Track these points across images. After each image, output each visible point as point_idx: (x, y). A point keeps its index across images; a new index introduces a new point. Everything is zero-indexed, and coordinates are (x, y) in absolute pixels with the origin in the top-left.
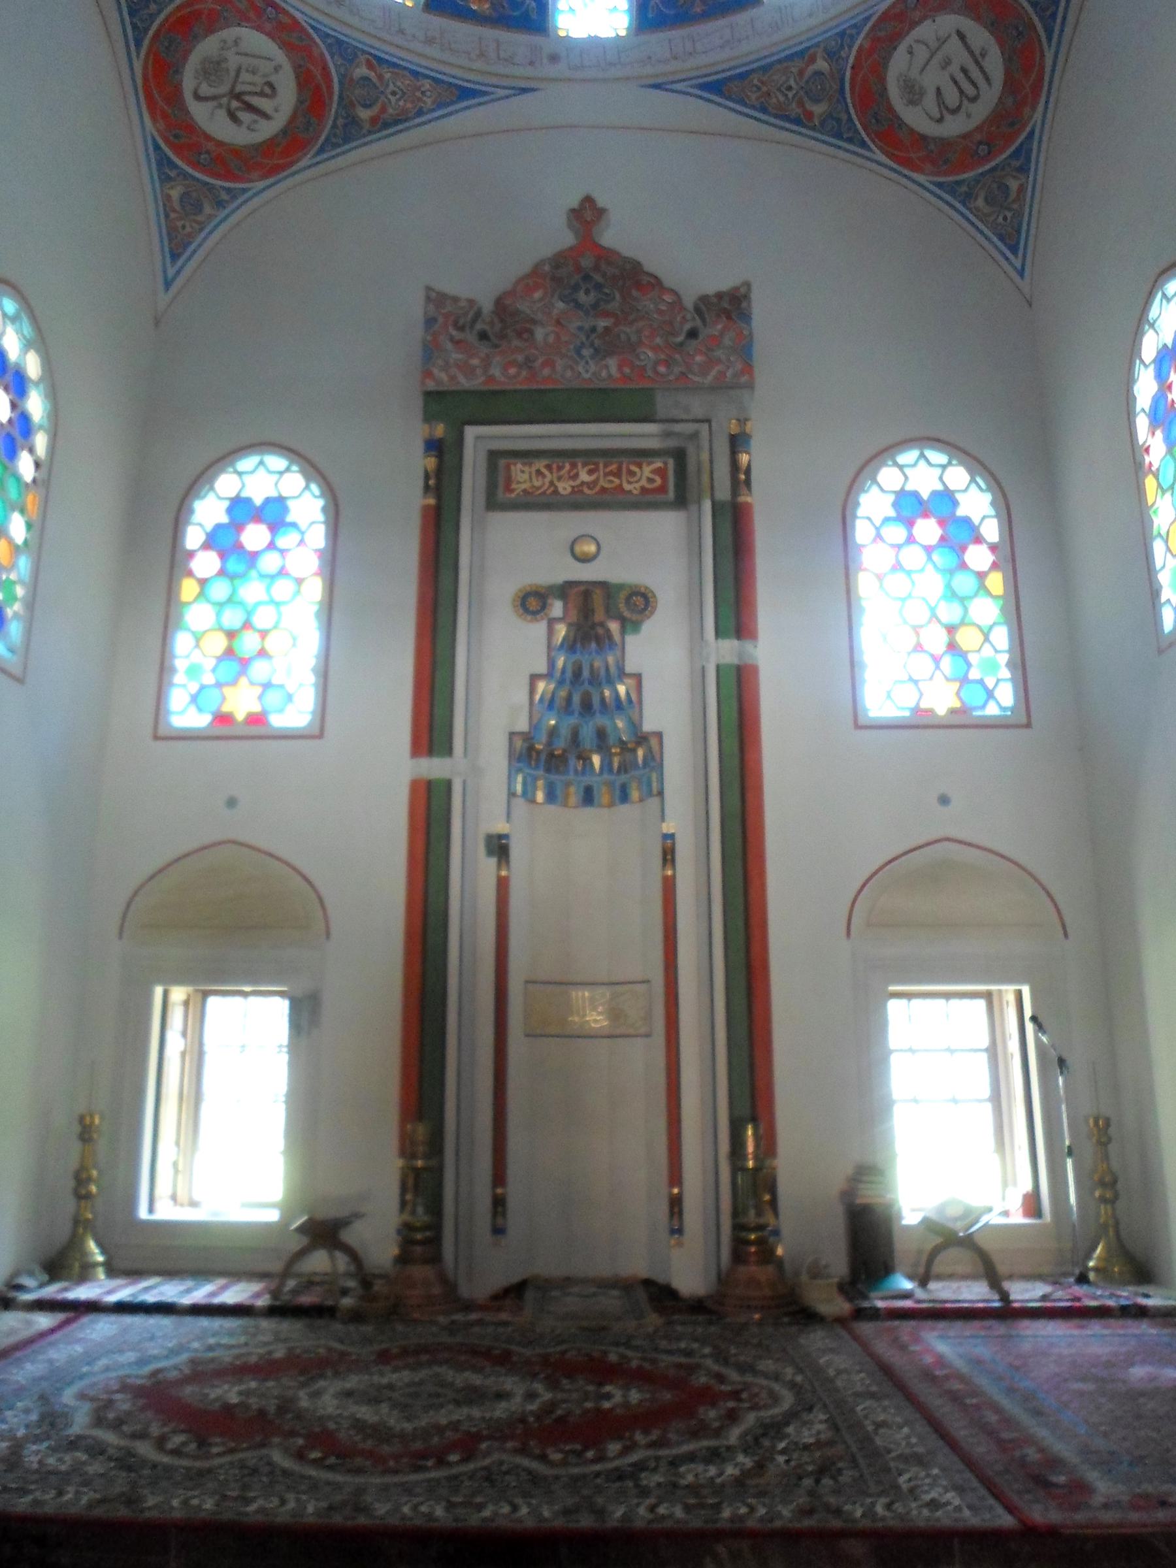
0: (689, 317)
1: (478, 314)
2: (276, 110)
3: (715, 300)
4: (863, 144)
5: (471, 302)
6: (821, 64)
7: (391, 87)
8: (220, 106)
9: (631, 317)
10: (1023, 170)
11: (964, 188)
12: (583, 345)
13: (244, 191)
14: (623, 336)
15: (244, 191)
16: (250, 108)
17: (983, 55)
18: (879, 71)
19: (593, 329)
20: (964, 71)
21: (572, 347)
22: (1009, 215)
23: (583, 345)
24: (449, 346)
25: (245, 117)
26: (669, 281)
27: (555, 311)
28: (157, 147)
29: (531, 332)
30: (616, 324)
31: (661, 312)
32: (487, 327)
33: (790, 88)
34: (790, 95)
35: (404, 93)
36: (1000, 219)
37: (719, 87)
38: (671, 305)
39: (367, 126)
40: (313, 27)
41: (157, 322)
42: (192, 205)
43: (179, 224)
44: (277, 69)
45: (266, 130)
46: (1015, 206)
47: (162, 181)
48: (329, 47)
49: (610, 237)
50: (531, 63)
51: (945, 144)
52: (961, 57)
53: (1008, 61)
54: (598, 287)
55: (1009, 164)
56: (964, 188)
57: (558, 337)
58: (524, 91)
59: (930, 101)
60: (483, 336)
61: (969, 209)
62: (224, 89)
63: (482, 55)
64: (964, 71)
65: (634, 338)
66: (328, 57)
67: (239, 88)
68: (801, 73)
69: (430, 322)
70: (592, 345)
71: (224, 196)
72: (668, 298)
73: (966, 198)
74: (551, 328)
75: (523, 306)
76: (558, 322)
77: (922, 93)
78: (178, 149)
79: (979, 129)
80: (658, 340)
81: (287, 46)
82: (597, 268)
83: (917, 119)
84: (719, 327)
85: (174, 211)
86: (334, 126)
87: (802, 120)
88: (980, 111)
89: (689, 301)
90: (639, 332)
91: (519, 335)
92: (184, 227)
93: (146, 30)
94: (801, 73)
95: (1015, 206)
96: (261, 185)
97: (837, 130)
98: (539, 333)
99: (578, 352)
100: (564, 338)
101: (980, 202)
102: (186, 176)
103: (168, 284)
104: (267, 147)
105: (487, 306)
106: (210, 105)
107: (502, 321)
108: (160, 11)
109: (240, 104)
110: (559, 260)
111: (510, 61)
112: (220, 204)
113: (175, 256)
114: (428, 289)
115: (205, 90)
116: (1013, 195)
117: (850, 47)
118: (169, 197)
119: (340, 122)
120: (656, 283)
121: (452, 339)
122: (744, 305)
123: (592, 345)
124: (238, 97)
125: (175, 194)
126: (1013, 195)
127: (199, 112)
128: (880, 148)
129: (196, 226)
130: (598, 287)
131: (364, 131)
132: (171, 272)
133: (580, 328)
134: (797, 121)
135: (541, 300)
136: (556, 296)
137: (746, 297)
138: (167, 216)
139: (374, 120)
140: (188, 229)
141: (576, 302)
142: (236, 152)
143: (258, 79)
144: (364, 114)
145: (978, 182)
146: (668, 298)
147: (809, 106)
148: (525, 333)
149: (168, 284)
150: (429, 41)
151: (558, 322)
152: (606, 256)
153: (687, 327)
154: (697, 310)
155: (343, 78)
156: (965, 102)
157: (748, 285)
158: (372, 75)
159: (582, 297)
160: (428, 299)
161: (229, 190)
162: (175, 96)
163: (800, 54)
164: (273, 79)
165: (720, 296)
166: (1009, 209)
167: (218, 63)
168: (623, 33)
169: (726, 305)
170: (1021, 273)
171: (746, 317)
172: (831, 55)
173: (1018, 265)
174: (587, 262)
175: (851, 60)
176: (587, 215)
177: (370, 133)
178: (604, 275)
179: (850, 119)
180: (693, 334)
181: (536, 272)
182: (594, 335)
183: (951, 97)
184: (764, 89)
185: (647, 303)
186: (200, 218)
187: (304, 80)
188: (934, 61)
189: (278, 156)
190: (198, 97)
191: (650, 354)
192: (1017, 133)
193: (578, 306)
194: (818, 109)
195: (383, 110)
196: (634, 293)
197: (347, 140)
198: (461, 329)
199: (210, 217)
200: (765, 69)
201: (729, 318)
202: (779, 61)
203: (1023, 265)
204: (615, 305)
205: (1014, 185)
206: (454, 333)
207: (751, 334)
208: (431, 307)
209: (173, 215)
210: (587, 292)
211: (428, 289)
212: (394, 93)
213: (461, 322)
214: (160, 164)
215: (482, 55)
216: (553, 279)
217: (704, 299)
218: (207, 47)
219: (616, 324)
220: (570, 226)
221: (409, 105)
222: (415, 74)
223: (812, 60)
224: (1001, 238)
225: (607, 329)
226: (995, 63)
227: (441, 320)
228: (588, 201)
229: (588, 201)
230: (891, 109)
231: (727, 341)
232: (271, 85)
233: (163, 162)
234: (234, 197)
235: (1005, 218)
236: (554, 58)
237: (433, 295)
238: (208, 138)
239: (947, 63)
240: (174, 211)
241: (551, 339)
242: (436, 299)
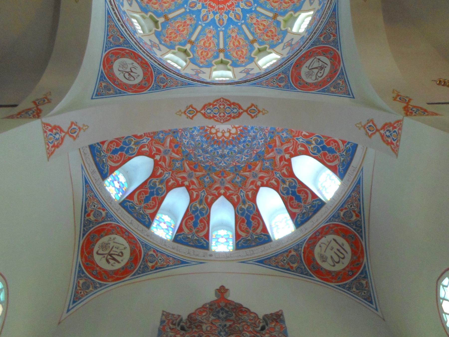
0: (261, 321)
1: (181, 320)
2: (122, 261)
3: (270, 316)
4: (311, 276)
5: (179, 316)
6: (293, 253)
7: (160, 258)
8: (104, 257)
9: (240, 321)
10: (365, 277)
11: (347, 286)
12: (221, 331)
13: (105, 285)
14: (237, 328)
15: (105, 285)
16: (114, 259)
17: (343, 245)
18: (312, 252)
19: (225, 325)
20: (338, 250)
21: (217, 331)
22: (365, 292)
23: (221, 331)
24: (169, 330)
25: (112, 261)
26: (252, 310)
27: (211, 319)
28: (80, 266)
29: (201, 326)
30: (234, 324)
31: (250, 320)
32: (184, 324)
33: (284, 260)
34: (285, 262)
35: (164, 260)
36: (363, 294)
37: (262, 262)
38: (255, 317)
39: (150, 268)
40: (139, 240)
41: (59, 323)
42: (86, 286)
43: (80, 291)
44: (125, 248)
45: (118, 266)
46: (367, 289)
47: (78, 277)
48: (142, 245)
49: (230, 298)
50: (204, 256)
51: (338, 273)
52: (336, 247)
53: (351, 246)
54: (227, 312)
55: (360, 276)
56: (347, 286)
57: (211, 327)
58: (201, 263)
59: (329, 260)
60: (183, 329)
61: (351, 292)
62: (107, 252)
63: (189, 253)
64: (338, 250)
65: (241, 329)
66: (142, 247)
67: (112, 252)
68: (287, 256)
69: (162, 322)
70: (225, 331)
71: (98, 285)
72: (253, 315)
73: (349, 289)
74: (208, 325)
75: (199, 318)
76: (212, 323)
77: (327, 258)
78: (86, 268)
79: (347, 267)
80: (251, 329)
81: (129, 242)
82: (226, 306)
83: (326, 266)
84: (273, 324)
85: (79, 286)
86: (140, 267)
87: (290, 269)
88: (347, 262)
89: (261, 316)
90: (243, 326)
91: (196, 327)
92: (81, 293)
93: (87, 232)
94: (287, 256)
95: (367, 289)
96: (111, 284)
97: (302, 272)
98: (204, 327)
99: (219, 333)
100: (214, 328)
101: (354, 289)
102: (86, 277)
103: (68, 310)
104: (116, 272)
105: (185, 317)
106: (101, 256)
107: (190, 322)
108: (93, 227)
109: (111, 257)
110: (212, 304)
111: (197, 255)
112: (96, 288)
113: (74, 302)
114: (163, 311)
115: (101, 252)
116: (365, 286)
117: (301, 248)
118: (79, 282)
119: (142, 267)
120: (247, 311)
121: (170, 328)
122: (281, 317)
123: (225, 331)
124: (111, 255)
125: (81, 282)
126: (365, 286)
127: (97, 258)
128: (316, 276)
129: (85, 293)
130: (227, 312)
131: (149, 270)
132: (71, 306)
133: (220, 325)
134: (288, 270)
135: (205, 315)
136: (211, 314)
137: (282, 314)
138: (76, 288)
139: (153, 267)
140: (82, 293)
141: (218, 316)
142: (106, 272)
143: (119, 251)
144: (150, 265)
145: (352, 283)
146: (253, 315)
147: (292, 265)
148: (199, 326)
149: (68, 310)
150: (173, 248)
151: (212, 323)
152: (230, 303)
153: (261, 325)
154: (264, 319)
155: (145, 253)
156: (341, 259)
157: (281, 310)
158: (155, 254)
159: (221, 315)
160: (163, 314)
161: (100, 284)
162: (90, 252)
163: (286, 251)
164: (123, 251)
165: (272, 314)
166: (365, 290)
167: (107, 244)
168: (231, 250)
169: (275, 317)
170: (376, 309)
171: (283, 321)
172: (295, 250)
173: (374, 306)
174: (222, 304)
175: (302, 251)
176: (222, 291)
177: (151, 271)
178: (229, 308)
179: (305, 268)
180: (263, 328)
181: (204, 307)
182: (225, 328)
183: (336, 259)
184: (276, 261)
185: (245, 317)
186: (87, 291)
187: (133, 252)
188: (328, 248)
189: (119, 275)
190: (97, 253)
191: (248, 334)
192: (361, 267)
193: (219, 318)
194: (295, 265)
195: (156, 263)
196: (240, 314)
197: (143, 272)
198: (175, 325)
199: (91, 291)
200: (276, 256)
201: (277, 322)
202: (280, 253)
203: (376, 307)
204: (232, 318)
205: (364, 282)
206: (171, 326)
207: (286, 327)
208: (164, 317)
209: (78, 288)
210: (222, 313)
211: (163, 311)
212: (160, 259)
213: (174, 323)
214: (79, 272)
215: (189, 253)
216: (210, 309)
217: (266, 315)
218: (105, 239)
219: (234, 324)
220: (216, 294)
221: (165, 263)
222: (168, 256)
223: (290, 252)
224: (365, 299)
225: (230, 326)
226: (347, 247)
227: (167, 321)
228: (222, 287)
229: (222, 287)
230: (317, 263)
231: (277, 329)
232: (122, 253)
233: (81, 271)
234: (101, 287)
235: (365, 293)
236: (211, 255)
237: (165, 313)
238: (98, 266)
239: (332, 249)
240: (79, 286)
241: (209, 329)
242: (166, 315)
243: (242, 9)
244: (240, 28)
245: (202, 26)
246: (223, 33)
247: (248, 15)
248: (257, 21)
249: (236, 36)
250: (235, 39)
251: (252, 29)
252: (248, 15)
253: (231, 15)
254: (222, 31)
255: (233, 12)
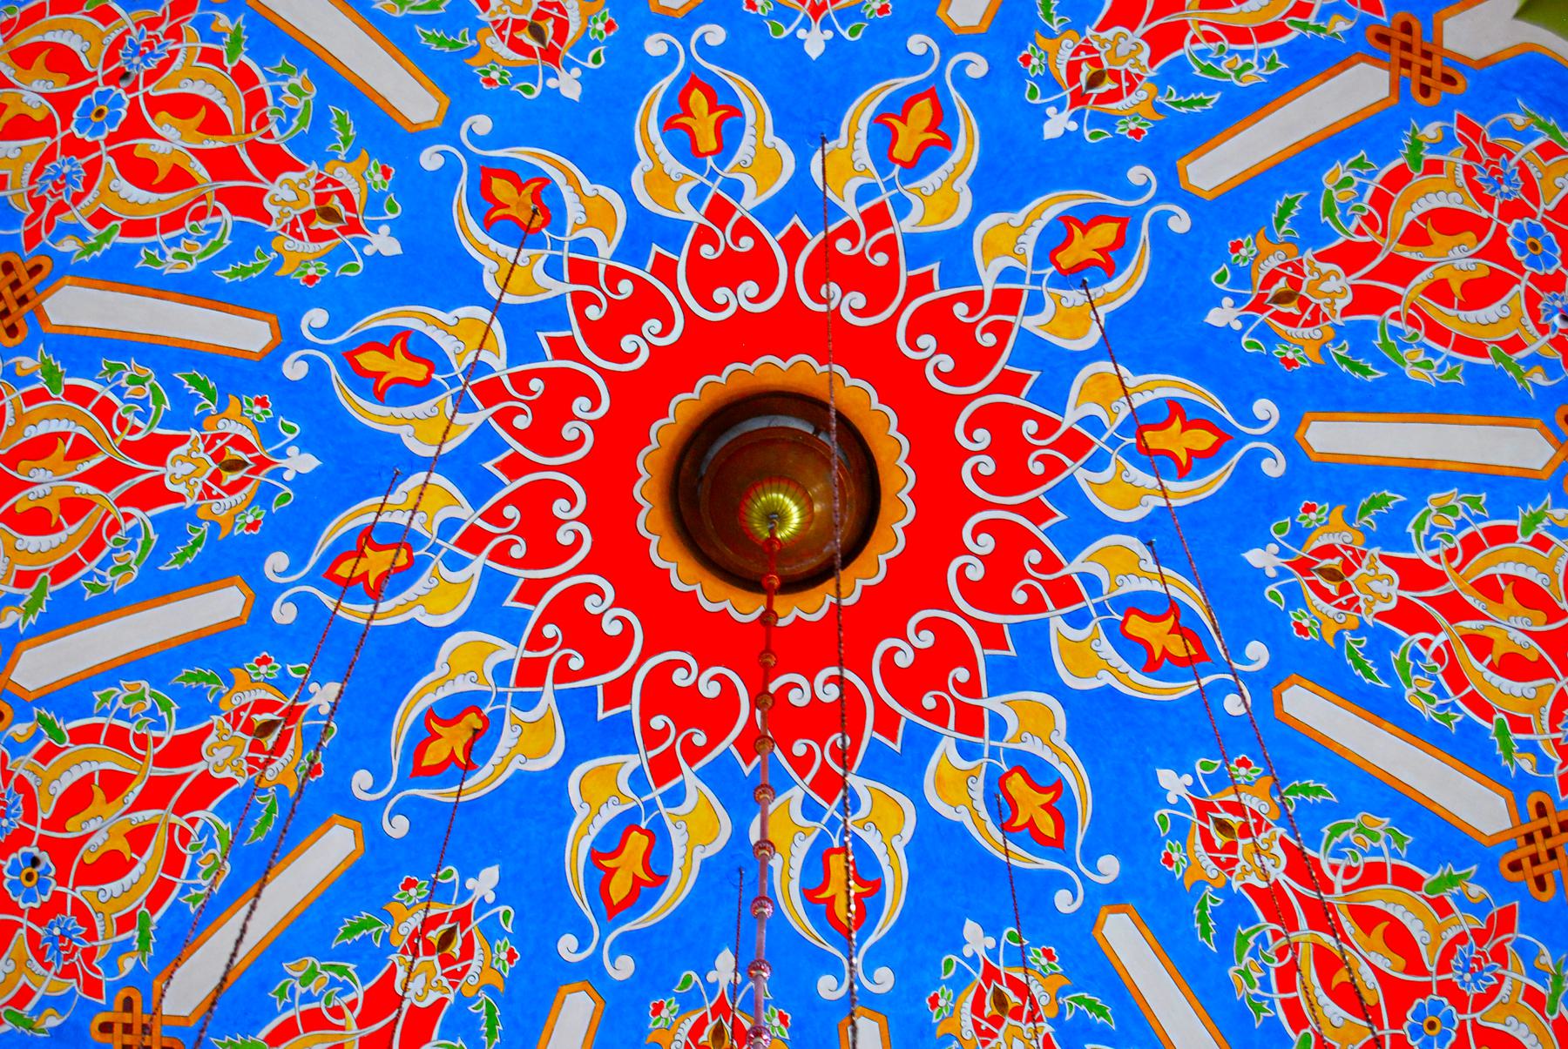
243: (1144, 530)
244: (1288, 753)
245: (874, 1004)
246: (1145, 920)
247: (1262, 558)
248: (1414, 574)
249: (1300, 866)
250: (1321, 917)
251: (1419, 694)
252: (1262, 558)
253: (1083, 659)
254: (1114, 896)
255: (1078, 621)
